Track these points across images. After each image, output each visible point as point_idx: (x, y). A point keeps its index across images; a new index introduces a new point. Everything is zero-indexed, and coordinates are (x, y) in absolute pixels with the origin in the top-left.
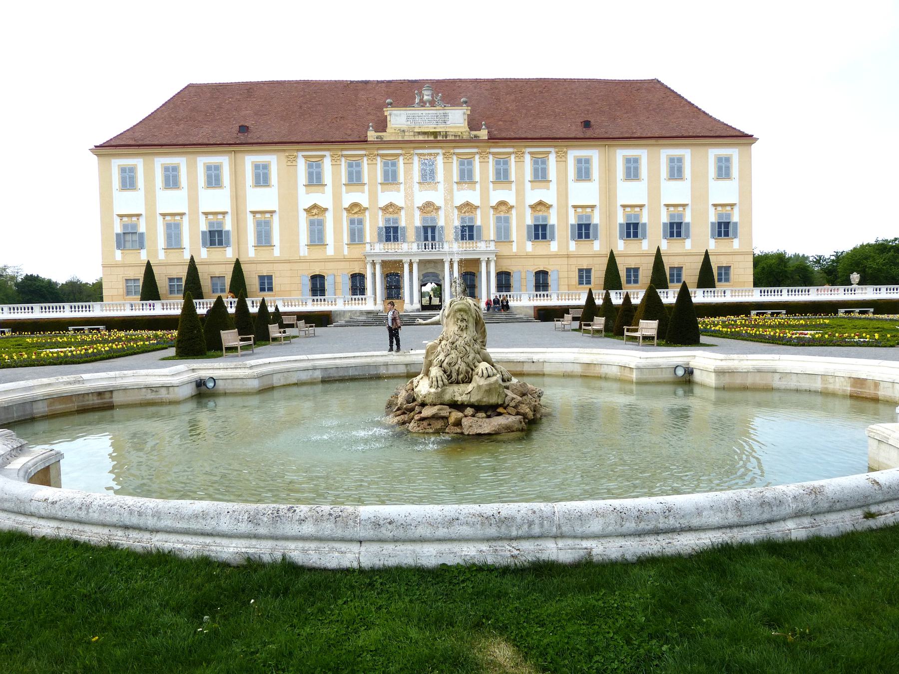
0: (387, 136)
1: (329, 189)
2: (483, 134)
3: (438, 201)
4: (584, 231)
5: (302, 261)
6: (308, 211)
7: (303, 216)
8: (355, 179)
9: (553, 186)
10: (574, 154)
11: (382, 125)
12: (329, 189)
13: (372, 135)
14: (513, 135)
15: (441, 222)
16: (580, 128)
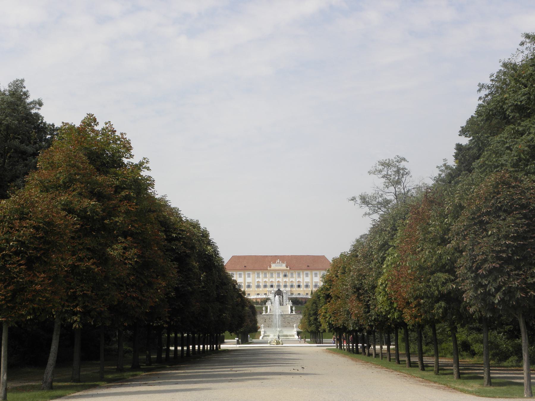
0: (271, 269)
1: (261, 278)
2: (289, 268)
3: (281, 281)
4: (307, 286)
5: (255, 291)
6: (257, 282)
7: (256, 283)
8: (266, 277)
9: (302, 278)
10: (305, 272)
11: (270, 267)
12: (261, 278)
13: (269, 269)
14: (294, 268)
15: (281, 284)
16: (307, 267)
